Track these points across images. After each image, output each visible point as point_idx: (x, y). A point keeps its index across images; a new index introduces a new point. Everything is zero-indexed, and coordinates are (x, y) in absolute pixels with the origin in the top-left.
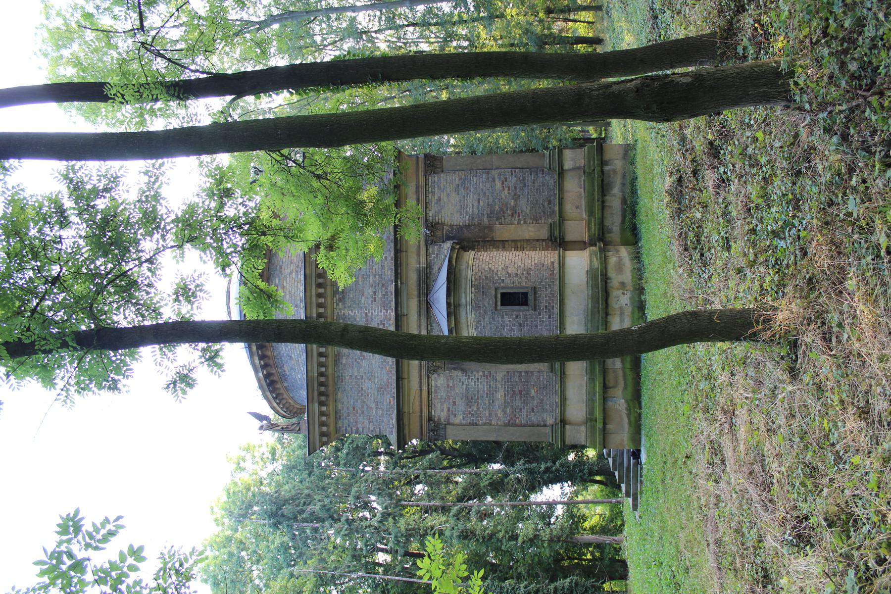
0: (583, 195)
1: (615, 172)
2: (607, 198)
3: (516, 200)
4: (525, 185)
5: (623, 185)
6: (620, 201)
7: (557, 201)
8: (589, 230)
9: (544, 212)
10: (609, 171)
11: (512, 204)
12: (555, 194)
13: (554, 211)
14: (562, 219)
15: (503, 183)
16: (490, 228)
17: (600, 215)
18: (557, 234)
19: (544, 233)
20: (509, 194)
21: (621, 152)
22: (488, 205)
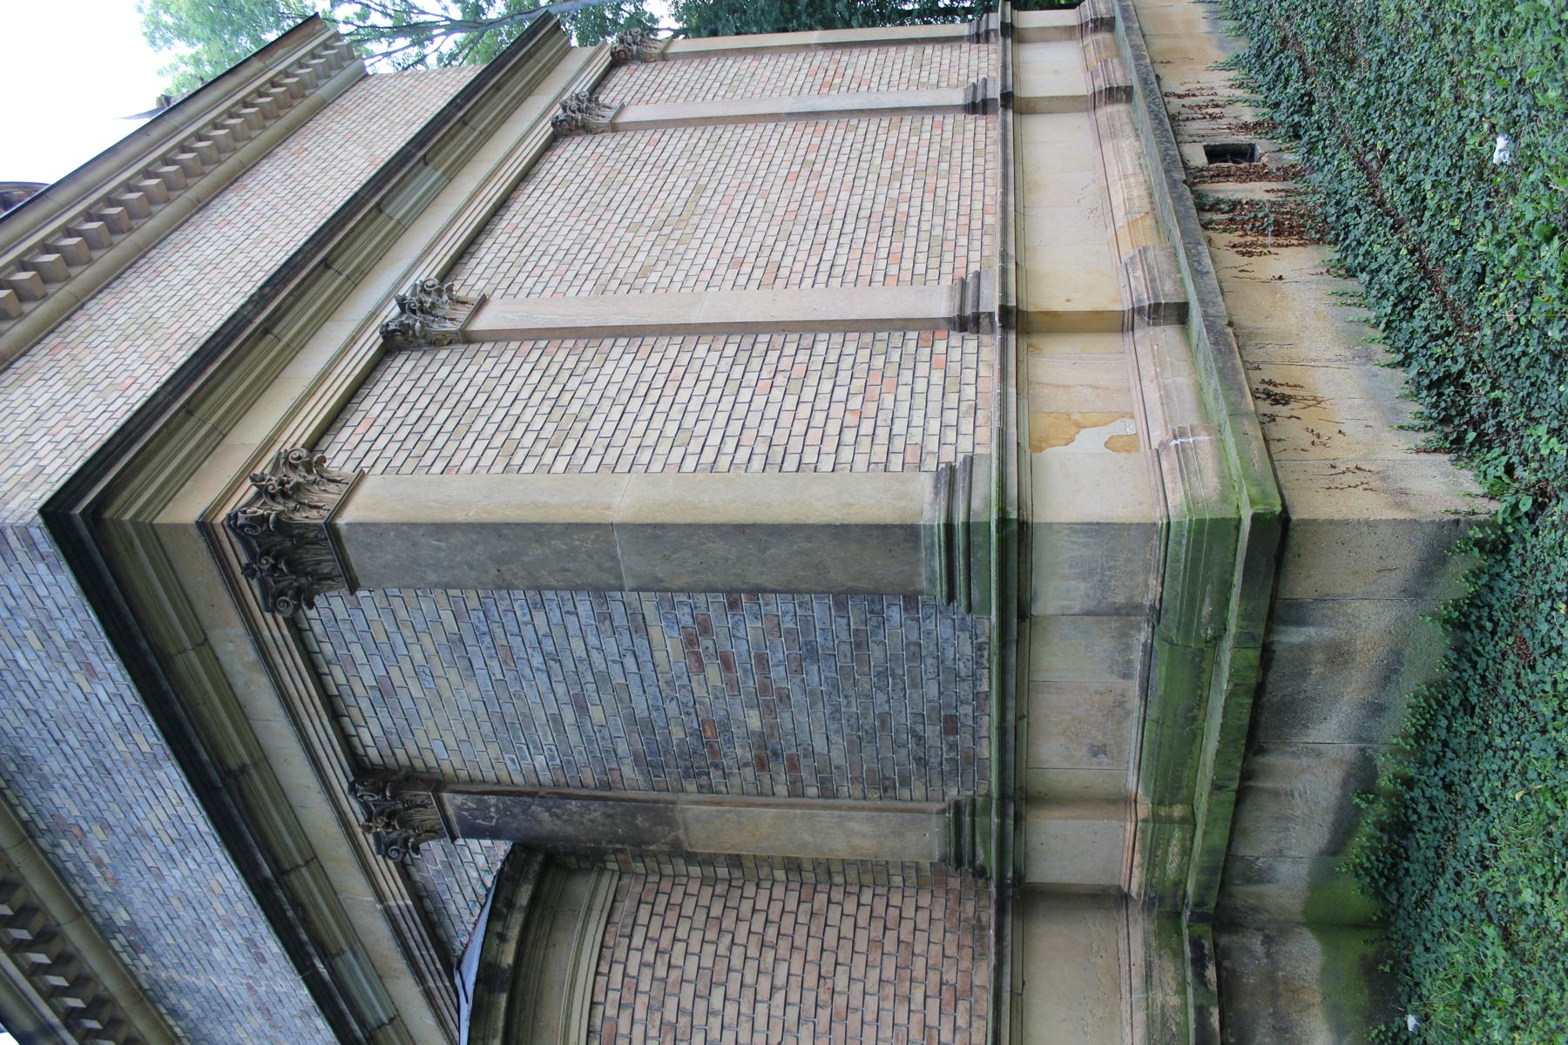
0: (1135, 702)
1: (1338, 655)
2: (1273, 760)
3: (768, 710)
4: (812, 653)
5: (1376, 709)
6: (1337, 774)
7: (990, 721)
8: (1153, 862)
9: (922, 762)
10: (1306, 647)
11: (754, 722)
12: (979, 699)
13: (972, 759)
14: (1019, 797)
15: (690, 642)
16: (661, 813)
17: (1219, 838)
18: (987, 855)
19: (926, 840)
20: (734, 685)
21: (1405, 558)
22: (632, 720)
